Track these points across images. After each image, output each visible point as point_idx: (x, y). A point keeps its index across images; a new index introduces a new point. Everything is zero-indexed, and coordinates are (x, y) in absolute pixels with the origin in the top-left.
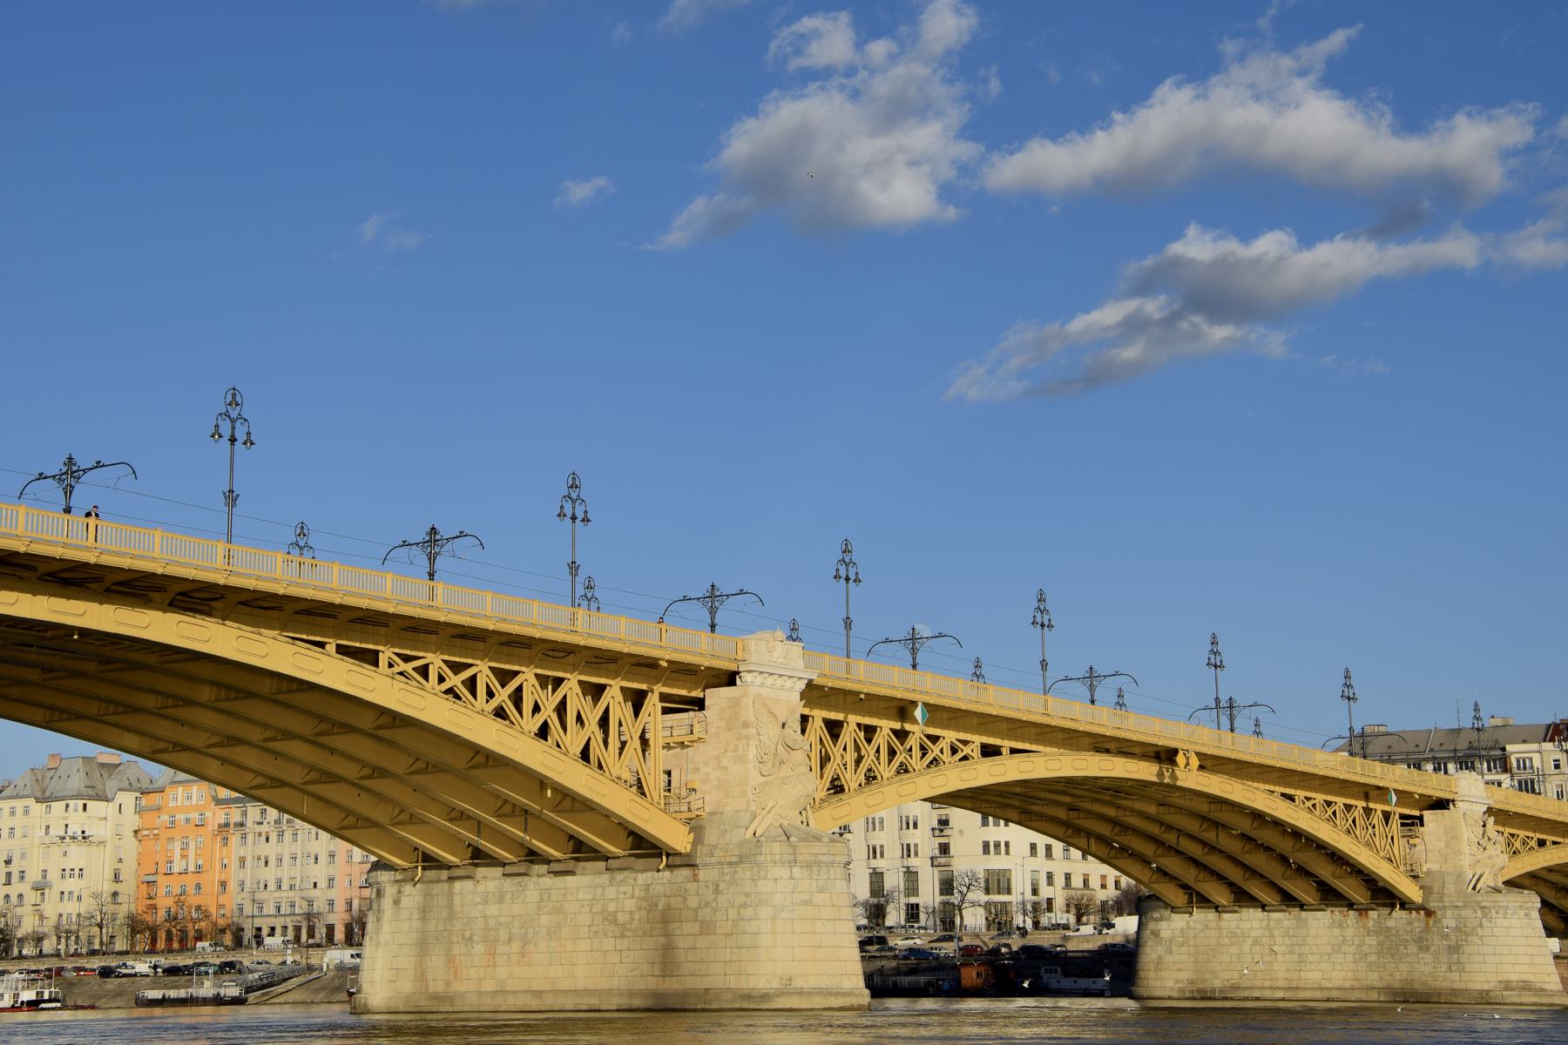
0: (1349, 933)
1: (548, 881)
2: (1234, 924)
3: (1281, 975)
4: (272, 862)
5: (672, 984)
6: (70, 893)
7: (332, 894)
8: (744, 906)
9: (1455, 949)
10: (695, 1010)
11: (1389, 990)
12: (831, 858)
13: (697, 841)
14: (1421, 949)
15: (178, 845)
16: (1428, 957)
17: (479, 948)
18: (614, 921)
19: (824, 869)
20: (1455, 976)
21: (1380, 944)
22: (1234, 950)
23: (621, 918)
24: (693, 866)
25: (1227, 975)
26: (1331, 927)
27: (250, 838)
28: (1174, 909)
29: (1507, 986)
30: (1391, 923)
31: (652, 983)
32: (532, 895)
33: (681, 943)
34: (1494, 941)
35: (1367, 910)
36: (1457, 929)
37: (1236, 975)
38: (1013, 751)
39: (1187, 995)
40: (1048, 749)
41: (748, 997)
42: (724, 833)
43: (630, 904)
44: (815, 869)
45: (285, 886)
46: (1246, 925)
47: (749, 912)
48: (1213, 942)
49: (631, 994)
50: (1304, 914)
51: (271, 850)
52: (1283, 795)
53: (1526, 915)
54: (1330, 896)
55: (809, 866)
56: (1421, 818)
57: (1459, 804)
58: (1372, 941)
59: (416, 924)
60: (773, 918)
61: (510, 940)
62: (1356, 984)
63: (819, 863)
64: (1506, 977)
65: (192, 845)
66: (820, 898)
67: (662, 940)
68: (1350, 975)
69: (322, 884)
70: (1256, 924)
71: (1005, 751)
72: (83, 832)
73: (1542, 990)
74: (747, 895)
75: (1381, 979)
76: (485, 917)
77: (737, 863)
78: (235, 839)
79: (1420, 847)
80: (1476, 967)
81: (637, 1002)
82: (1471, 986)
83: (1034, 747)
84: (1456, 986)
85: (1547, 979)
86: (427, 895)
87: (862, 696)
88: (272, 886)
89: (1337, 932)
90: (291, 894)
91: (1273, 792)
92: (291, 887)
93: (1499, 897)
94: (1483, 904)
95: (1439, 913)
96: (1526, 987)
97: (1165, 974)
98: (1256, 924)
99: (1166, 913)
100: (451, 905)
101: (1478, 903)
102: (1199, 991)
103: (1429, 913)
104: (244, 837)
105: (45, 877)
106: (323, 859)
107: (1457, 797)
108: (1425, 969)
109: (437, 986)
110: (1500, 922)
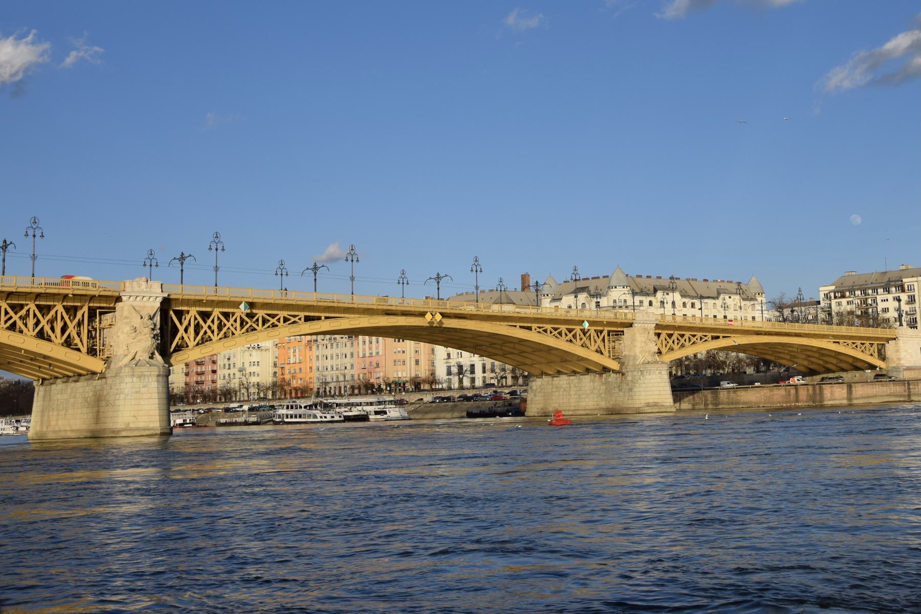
0: (596, 384)
1: (73, 384)
2: (557, 382)
3: (573, 404)
4: (329, 358)
5: (98, 427)
6: (254, 373)
7: (353, 372)
8: (116, 394)
9: (631, 390)
10: (101, 437)
11: (607, 409)
12: (149, 373)
13: (108, 368)
14: (619, 390)
15: (292, 350)
16: (621, 394)
17: (55, 413)
18: (87, 401)
19: (147, 378)
20: (630, 402)
21: (606, 389)
22: (557, 394)
23: (89, 399)
24: (105, 378)
25: (554, 405)
26: (590, 382)
27: (320, 346)
28: (538, 377)
29: (648, 405)
30: (610, 379)
31: (93, 427)
32: (69, 391)
33: (102, 410)
34: (644, 385)
35: (602, 374)
36: (632, 381)
37: (557, 405)
38: (326, 318)
39: (540, 415)
40: (352, 316)
41: (113, 432)
42: (116, 363)
43: (91, 394)
44: (143, 378)
45: (335, 369)
46: (561, 383)
47: (117, 397)
48: (550, 391)
49: (88, 431)
50: (581, 376)
51: (328, 352)
52: (521, 327)
53: (659, 373)
54: (588, 371)
55: (140, 377)
56: (623, 331)
57: (636, 325)
58: (603, 387)
59: (42, 402)
60: (125, 399)
61: (63, 409)
62: (598, 407)
63: (144, 376)
64: (647, 401)
65: (297, 350)
66: (143, 390)
67: (97, 408)
68: (595, 403)
69: (349, 367)
70: (565, 382)
71: (323, 318)
72: (258, 345)
73: (662, 406)
74: (117, 389)
75: (606, 404)
76: (58, 400)
77: (116, 376)
78: (314, 348)
79: (622, 345)
80: (637, 397)
81: (89, 435)
82: (635, 406)
83: (342, 315)
84: (630, 406)
85: (665, 401)
86: (45, 391)
87: (204, 301)
88: (329, 369)
89: (592, 384)
90: (337, 372)
91: (515, 326)
92: (337, 369)
93: (648, 366)
94: (641, 369)
95: (626, 374)
96: (655, 405)
97: (533, 406)
98: (565, 382)
99: (535, 378)
100: (50, 395)
101: (639, 369)
102: (544, 413)
103: (623, 374)
104: (318, 346)
105: (243, 365)
106: (349, 356)
107: (634, 322)
108: (621, 399)
109: (45, 429)
110: (648, 377)
